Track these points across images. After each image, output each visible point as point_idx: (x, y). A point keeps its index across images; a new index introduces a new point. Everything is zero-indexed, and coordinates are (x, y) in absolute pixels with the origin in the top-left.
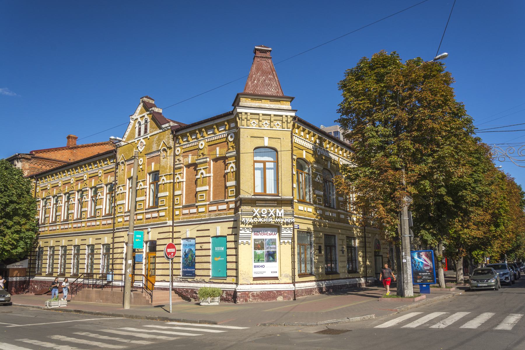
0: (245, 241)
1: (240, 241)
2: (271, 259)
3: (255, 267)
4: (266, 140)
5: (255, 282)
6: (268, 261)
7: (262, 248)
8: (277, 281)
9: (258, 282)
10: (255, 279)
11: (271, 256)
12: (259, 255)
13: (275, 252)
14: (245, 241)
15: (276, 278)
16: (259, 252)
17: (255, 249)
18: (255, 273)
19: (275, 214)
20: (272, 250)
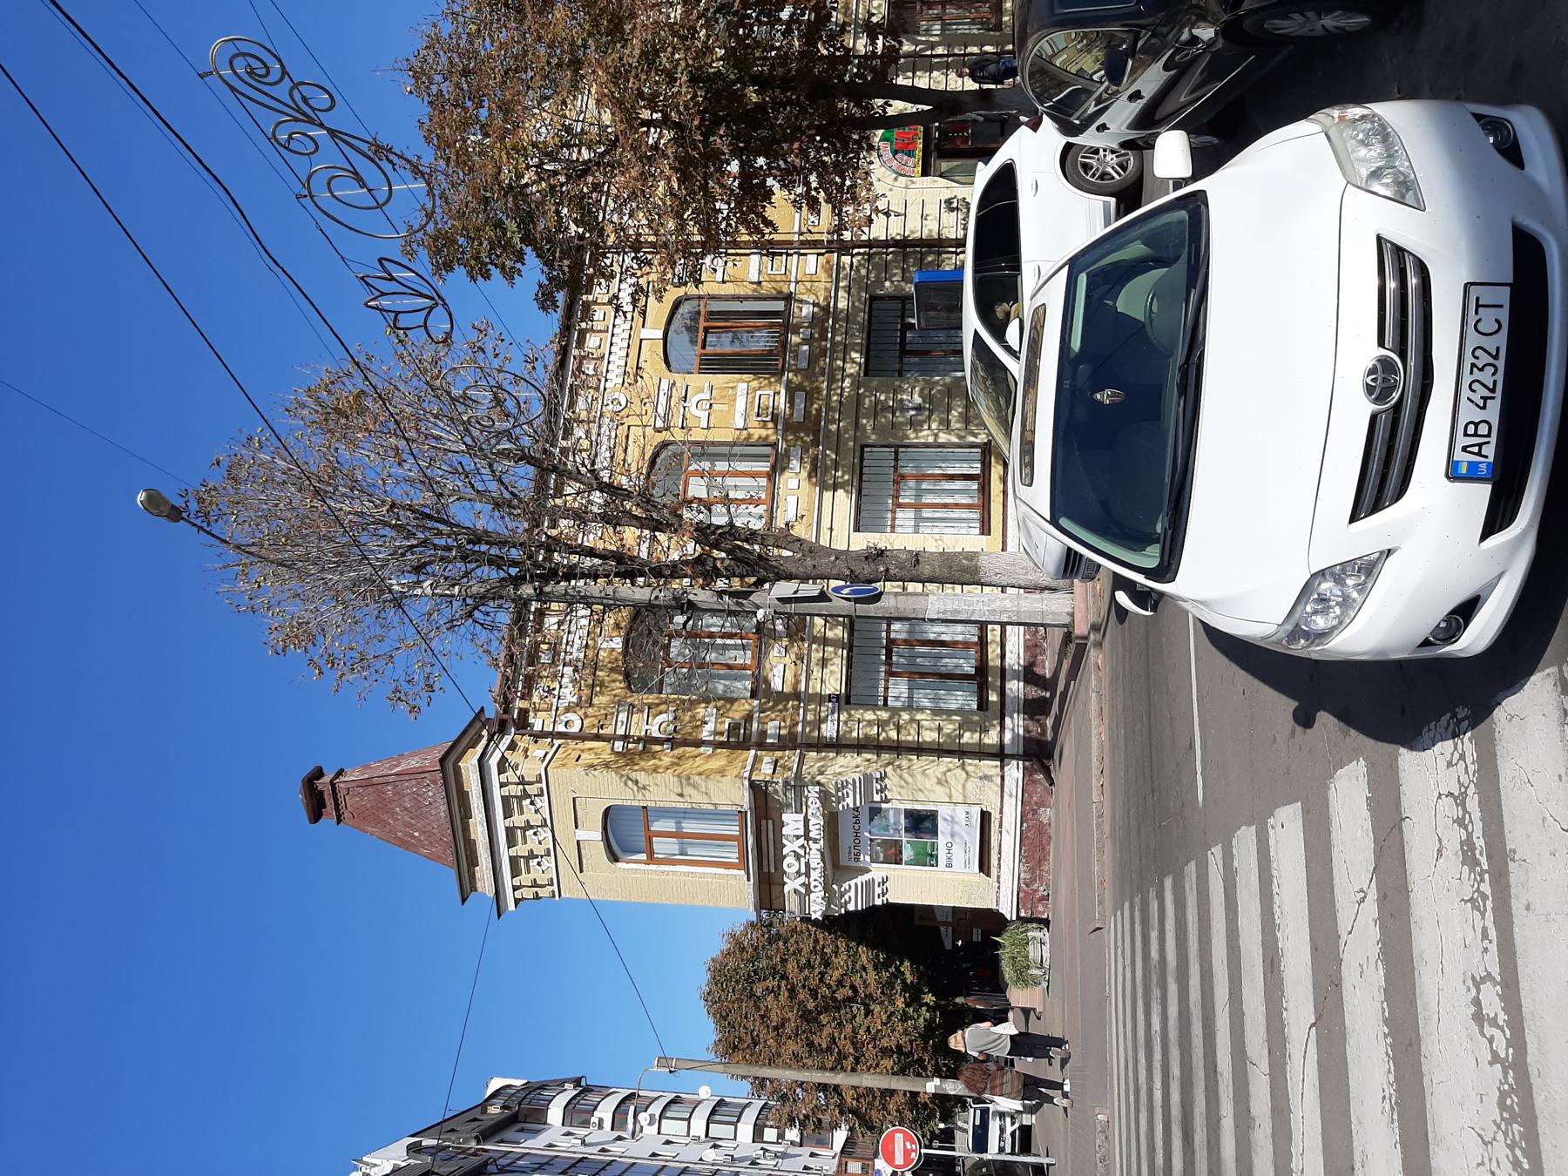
0: (878, 890)
1: (878, 902)
2: (927, 824)
3: (949, 866)
4: (581, 834)
5: (994, 871)
6: (934, 832)
7: (897, 845)
8: (995, 816)
9: (994, 862)
10: (984, 867)
11: (922, 823)
12: (916, 855)
13: (910, 814)
14: (878, 890)
15: (985, 817)
16: (907, 853)
17: (899, 862)
18: (967, 863)
19: (798, 837)
20: (903, 821)
